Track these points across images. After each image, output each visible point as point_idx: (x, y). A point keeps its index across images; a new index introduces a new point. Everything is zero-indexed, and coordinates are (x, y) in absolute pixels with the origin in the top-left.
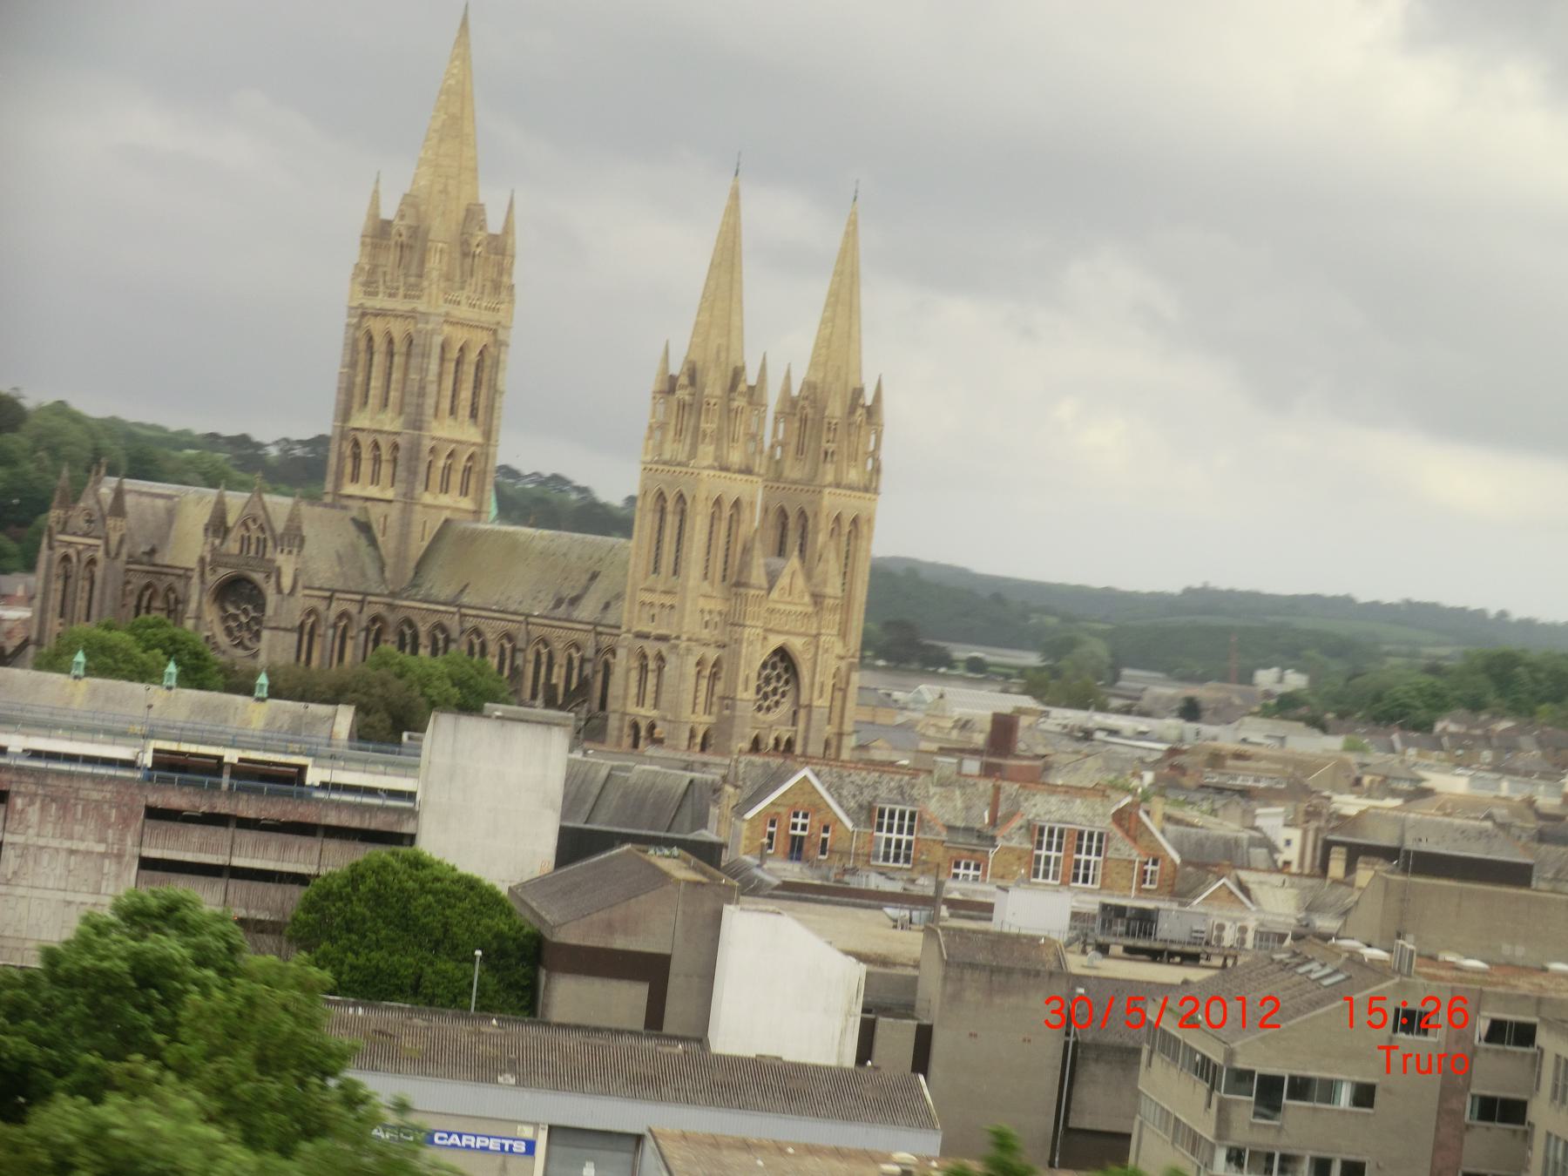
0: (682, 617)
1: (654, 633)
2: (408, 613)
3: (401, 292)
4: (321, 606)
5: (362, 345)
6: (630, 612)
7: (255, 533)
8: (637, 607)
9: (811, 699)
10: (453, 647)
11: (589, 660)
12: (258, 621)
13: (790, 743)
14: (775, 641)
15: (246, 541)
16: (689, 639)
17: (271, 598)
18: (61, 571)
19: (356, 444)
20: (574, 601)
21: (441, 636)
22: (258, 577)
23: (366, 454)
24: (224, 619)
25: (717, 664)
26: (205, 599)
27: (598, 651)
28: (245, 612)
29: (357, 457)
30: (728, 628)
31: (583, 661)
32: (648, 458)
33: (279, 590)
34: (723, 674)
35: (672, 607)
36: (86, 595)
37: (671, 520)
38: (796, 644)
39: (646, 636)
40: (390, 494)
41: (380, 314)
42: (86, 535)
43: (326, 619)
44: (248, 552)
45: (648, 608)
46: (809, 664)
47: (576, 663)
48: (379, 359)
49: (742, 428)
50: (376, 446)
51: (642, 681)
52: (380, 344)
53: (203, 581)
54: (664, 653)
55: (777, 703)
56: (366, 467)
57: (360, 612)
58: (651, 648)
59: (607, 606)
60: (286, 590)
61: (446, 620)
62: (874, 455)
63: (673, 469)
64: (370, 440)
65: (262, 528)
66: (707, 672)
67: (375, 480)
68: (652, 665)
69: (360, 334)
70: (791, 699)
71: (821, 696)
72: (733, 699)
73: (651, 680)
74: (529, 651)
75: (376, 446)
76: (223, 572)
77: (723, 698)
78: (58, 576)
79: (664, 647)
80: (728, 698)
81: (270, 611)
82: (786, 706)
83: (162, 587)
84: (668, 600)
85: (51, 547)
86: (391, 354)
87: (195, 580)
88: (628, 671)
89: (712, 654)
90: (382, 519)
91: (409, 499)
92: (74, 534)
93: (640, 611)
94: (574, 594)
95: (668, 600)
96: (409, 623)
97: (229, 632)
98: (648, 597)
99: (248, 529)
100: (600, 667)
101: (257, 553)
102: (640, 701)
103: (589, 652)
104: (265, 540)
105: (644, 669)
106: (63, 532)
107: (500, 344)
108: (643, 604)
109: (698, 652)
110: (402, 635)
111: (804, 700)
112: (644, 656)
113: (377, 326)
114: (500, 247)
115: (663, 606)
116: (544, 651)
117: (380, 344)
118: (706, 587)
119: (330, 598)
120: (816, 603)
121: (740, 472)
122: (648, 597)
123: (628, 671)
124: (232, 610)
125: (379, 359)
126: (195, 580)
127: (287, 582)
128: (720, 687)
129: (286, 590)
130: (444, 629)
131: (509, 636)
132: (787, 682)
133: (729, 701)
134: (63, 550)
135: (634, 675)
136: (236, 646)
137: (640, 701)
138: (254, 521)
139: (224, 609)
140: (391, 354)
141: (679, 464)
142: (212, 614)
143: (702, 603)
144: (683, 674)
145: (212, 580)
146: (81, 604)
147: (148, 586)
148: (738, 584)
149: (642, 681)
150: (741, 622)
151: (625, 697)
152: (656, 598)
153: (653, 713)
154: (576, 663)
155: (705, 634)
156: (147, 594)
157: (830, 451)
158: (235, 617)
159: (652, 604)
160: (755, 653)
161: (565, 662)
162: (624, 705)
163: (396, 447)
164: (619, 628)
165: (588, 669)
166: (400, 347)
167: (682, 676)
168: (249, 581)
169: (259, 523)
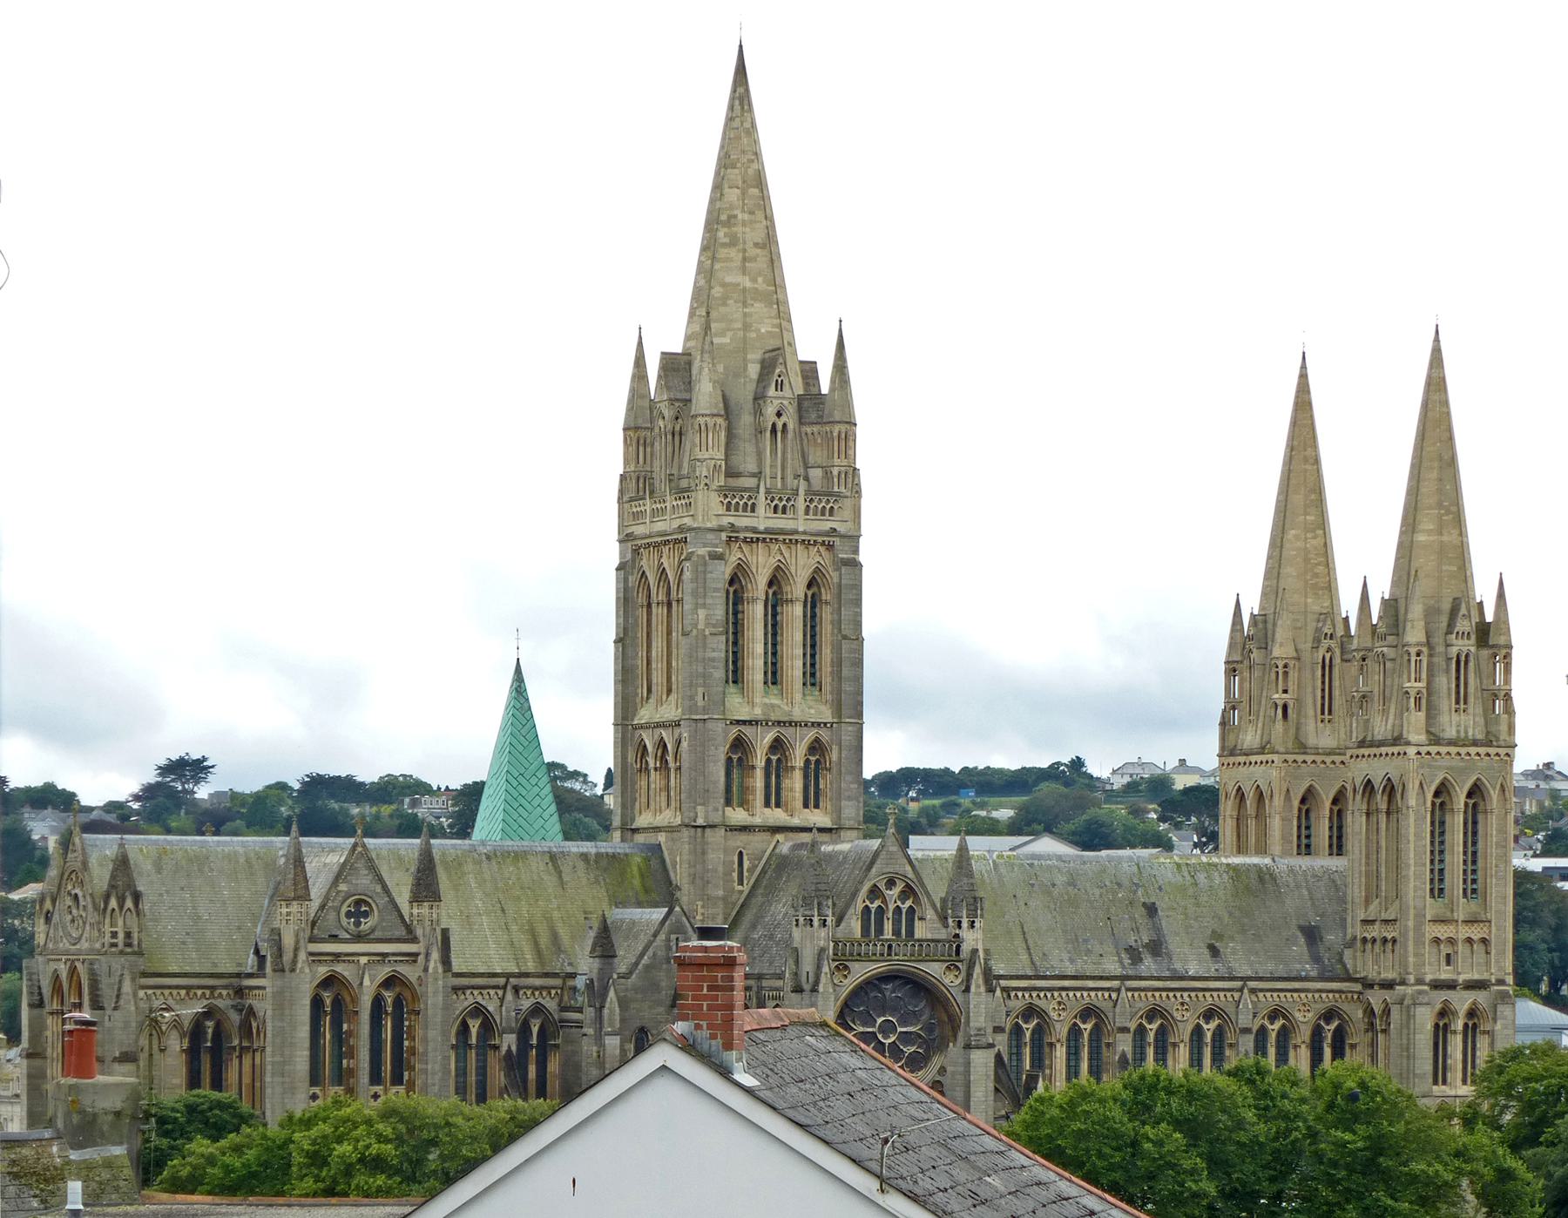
1: (1461, 979)
3: (801, 504)
35: (1484, 941)
37: (1456, 822)
39: (1451, 986)
41: (769, 537)
44: (880, 930)
63: (1463, 751)
67: (774, 797)
76: (861, 971)
79: (1481, 997)
84: (1476, 933)
95: (1476, 933)
98: (1443, 932)
101: (896, 932)
113: (762, 564)
115: (1469, 940)
122: (1443, 932)
137: (1440, 1073)
140: (775, 604)
141: (1475, 743)
159: (1451, 941)
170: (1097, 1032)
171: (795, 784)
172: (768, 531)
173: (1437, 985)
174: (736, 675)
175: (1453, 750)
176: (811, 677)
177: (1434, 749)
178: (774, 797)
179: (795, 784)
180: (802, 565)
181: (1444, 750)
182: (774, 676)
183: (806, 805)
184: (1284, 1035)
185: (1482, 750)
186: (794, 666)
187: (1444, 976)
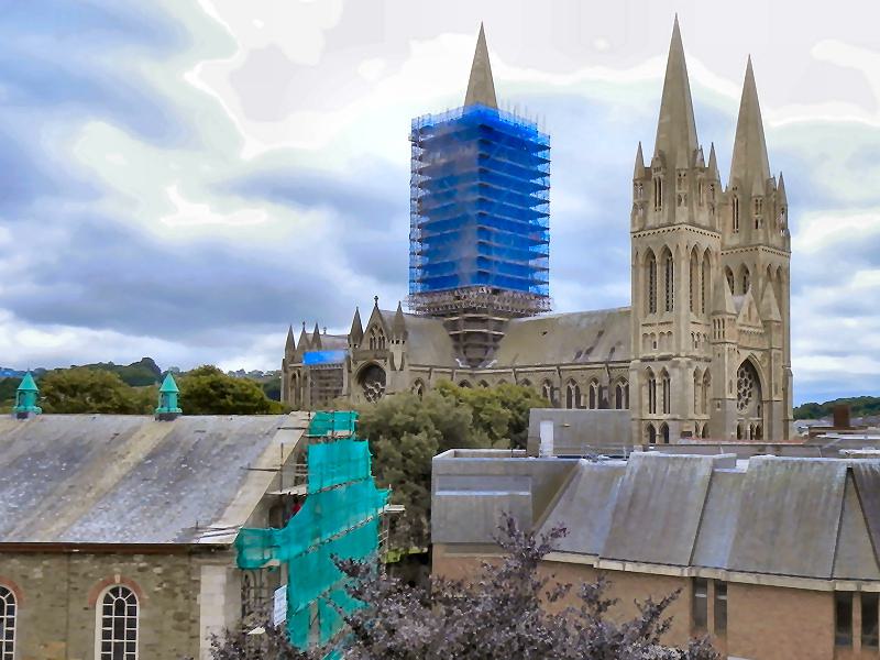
0: (679, 339)
4: (425, 377)
8: (641, 338)
11: (606, 388)
12: (382, 390)
13: (759, 430)
14: (745, 355)
17: (389, 373)
20: (589, 352)
22: (381, 362)
24: (366, 394)
25: (707, 374)
26: (352, 384)
28: (377, 386)
30: (712, 347)
31: (601, 389)
32: (637, 229)
33: (393, 368)
34: (711, 382)
38: (758, 355)
43: (429, 385)
45: (650, 338)
46: (767, 371)
47: (596, 391)
49: (705, 197)
51: (652, 395)
53: (350, 371)
54: (668, 369)
55: (747, 401)
57: (452, 379)
58: (656, 368)
59: (613, 350)
60: (398, 368)
66: (701, 381)
71: (776, 393)
73: (659, 391)
81: (388, 382)
82: (753, 404)
84: (665, 329)
87: (345, 371)
89: (703, 367)
94: (588, 347)
95: (665, 329)
98: (648, 330)
100: (614, 392)
102: (652, 409)
103: (605, 383)
105: (652, 384)
106: (292, 362)
109: (696, 364)
111: (765, 397)
112: (652, 374)
118: (693, 317)
119: (430, 372)
122: (648, 330)
123: (641, 386)
124: (369, 387)
126: (345, 371)
127: (397, 362)
128: (710, 391)
129: (398, 368)
132: (751, 386)
133: (719, 402)
135: (645, 390)
137: (652, 409)
139: (365, 387)
143: (693, 328)
144: (683, 381)
149: (652, 395)
151: (641, 407)
153: (665, 416)
154: (596, 391)
160: (732, 364)
161: (588, 392)
162: (641, 414)
165: (605, 394)
167: (685, 385)
168: (377, 367)
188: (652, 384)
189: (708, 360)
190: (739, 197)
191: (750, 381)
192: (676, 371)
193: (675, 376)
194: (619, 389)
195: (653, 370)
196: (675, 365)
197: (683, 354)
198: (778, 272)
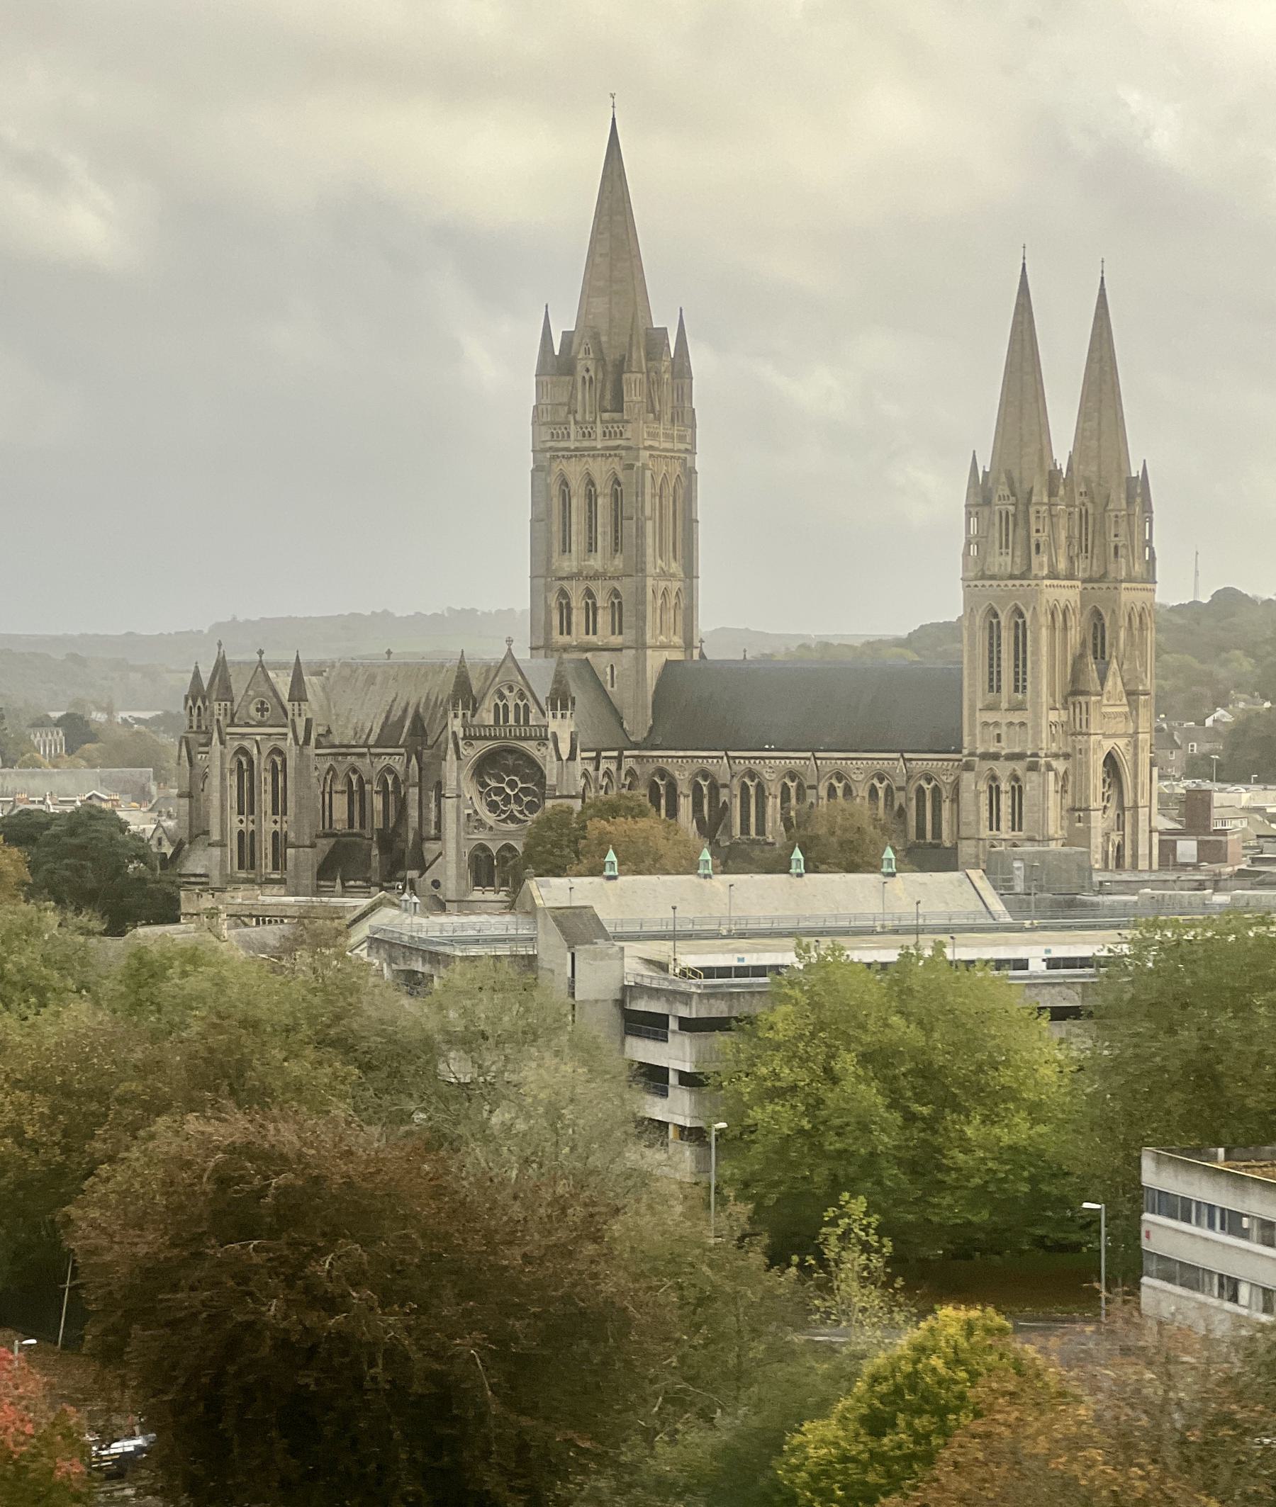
2: (661, 763)
3: (599, 430)
5: (555, 490)
6: (972, 734)
7: (512, 700)
8: (978, 729)
9: (1136, 802)
10: (811, 797)
11: (900, 789)
14: (1108, 745)
15: (500, 713)
16: (1046, 756)
17: (551, 770)
18: (235, 766)
19: (563, 593)
21: (704, 784)
22: (530, 747)
23: (577, 602)
27: (909, 778)
28: (512, 785)
29: (565, 610)
31: (889, 790)
34: (1069, 788)
35: (1023, 724)
36: (269, 788)
39: (995, 757)
40: (617, 640)
41: (578, 453)
42: (260, 725)
43: (597, 779)
44: (506, 720)
45: (991, 728)
48: (578, 503)
50: (589, 594)
52: (577, 486)
54: (1019, 773)
56: (578, 617)
57: (619, 768)
58: (1003, 770)
60: (565, 757)
61: (709, 765)
62: (1148, 543)
63: (1002, 583)
64: (582, 586)
65: (522, 696)
68: (1005, 786)
69: (553, 480)
70: (1115, 805)
72: (1087, 809)
73: (1005, 802)
74: (820, 788)
75: (589, 594)
76: (482, 747)
77: (1074, 809)
78: (231, 771)
79: (1019, 767)
80: (1080, 810)
81: (551, 780)
83: (341, 769)
84: (1016, 717)
85: (222, 742)
86: (591, 498)
88: (977, 794)
90: (608, 670)
91: (641, 646)
92: (248, 725)
93: (982, 733)
96: (662, 773)
97: (493, 807)
99: (502, 696)
101: (517, 720)
102: (995, 823)
104: (526, 707)
105: (995, 792)
106: (232, 724)
107: (690, 473)
108: (986, 724)
110: (654, 787)
111: (1128, 802)
112: (994, 778)
113: (575, 471)
114: (681, 369)
115: (1011, 724)
116: (839, 787)
117: (577, 486)
120: (1129, 704)
121: (1067, 578)
122: (990, 717)
123: (977, 794)
124: (493, 784)
125: (578, 503)
129: (565, 757)
130: (705, 774)
131: (792, 775)
134: (236, 743)
135: (984, 799)
136: (504, 821)
138: (511, 689)
139: (484, 785)
140: (591, 498)
141: (1012, 577)
142: (470, 790)
145: (472, 753)
146: (267, 798)
147: (331, 768)
148: (1075, 693)
150: (1084, 730)
151: (978, 822)
152: (1002, 717)
155: (1054, 748)
156: (329, 777)
157: (1120, 544)
158: (499, 791)
159: (996, 724)
163: (616, 594)
164: (960, 752)
166: (603, 486)
169: (516, 690)
170: (800, 787)
171: (603, 619)
172: (576, 449)
173: (986, 756)
174: (566, 548)
175: (994, 583)
176: (617, 545)
177: (979, 583)
178: (591, 627)
179: (603, 619)
180: (601, 470)
181: (987, 583)
182: (591, 547)
183: (613, 633)
184: (936, 790)
185: (1017, 582)
186: (604, 541)
187: (992, 750)
188: (995, 792)
189: (1067, 756)
190: (1090, 506)
191: (1108, 780)
192: (1033, 776)
193: (1031, 783)
194: (920, 791)
195: (998, 773)
196: (1033, 767)
197: (1042, 754)
198: (1140, 616)
